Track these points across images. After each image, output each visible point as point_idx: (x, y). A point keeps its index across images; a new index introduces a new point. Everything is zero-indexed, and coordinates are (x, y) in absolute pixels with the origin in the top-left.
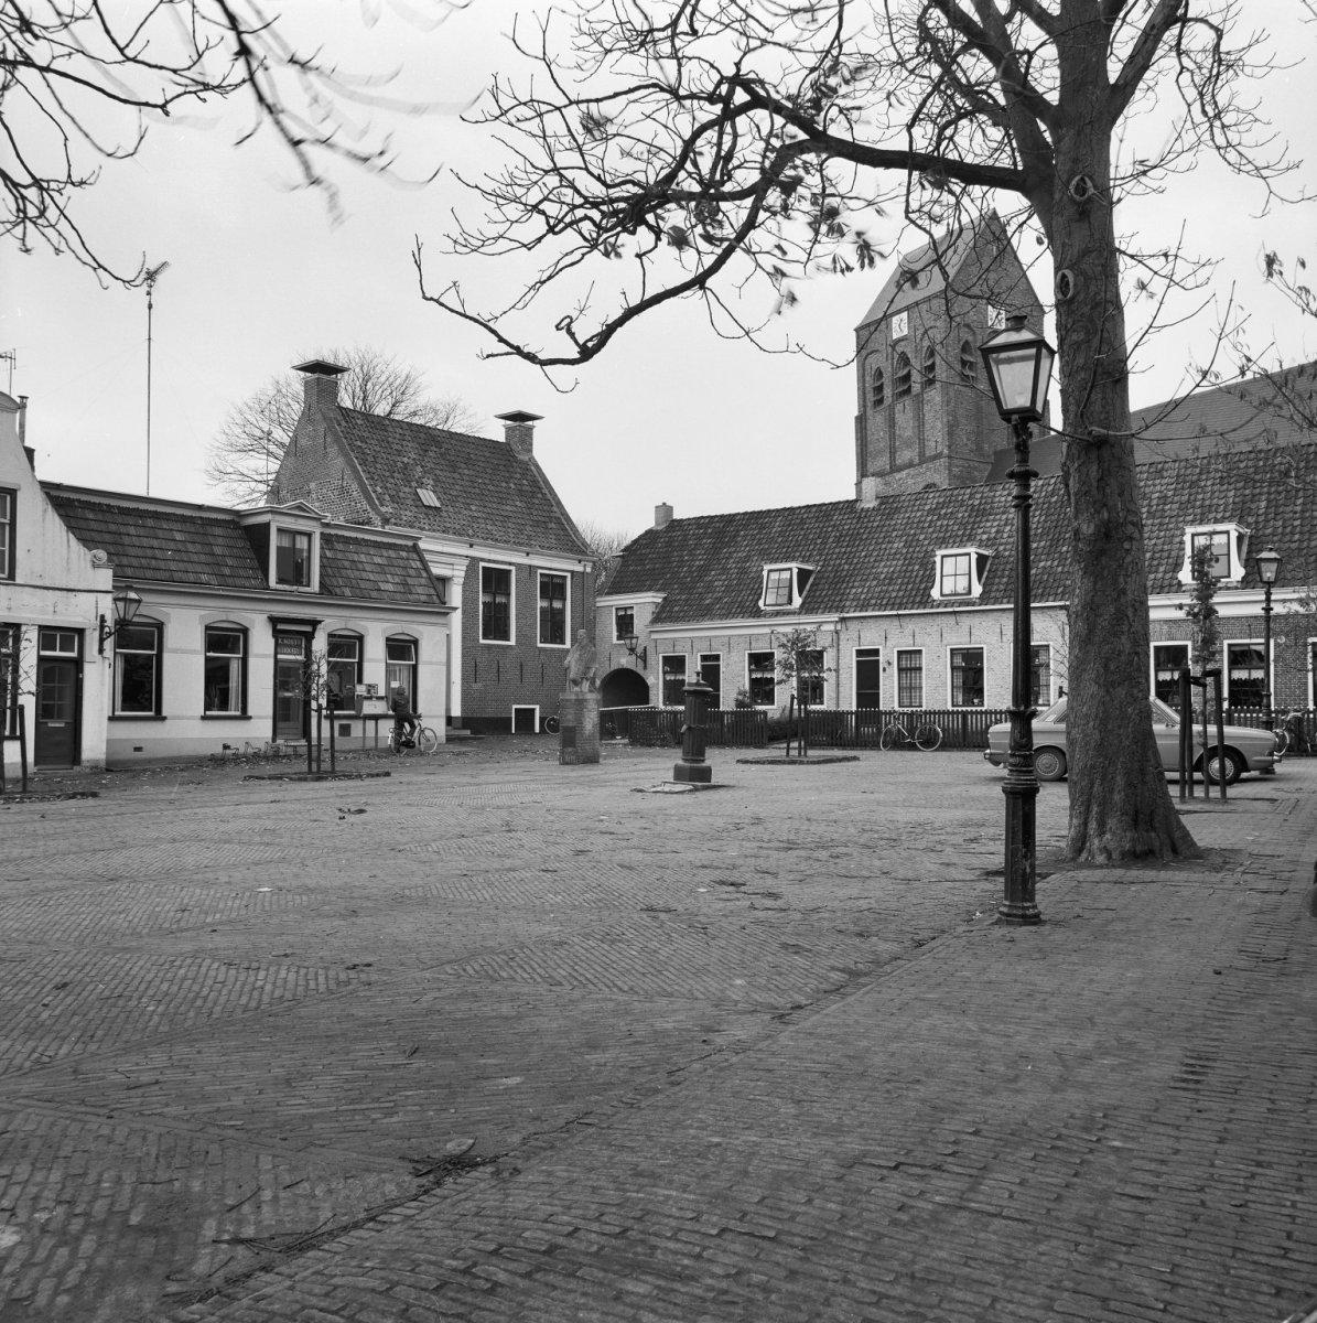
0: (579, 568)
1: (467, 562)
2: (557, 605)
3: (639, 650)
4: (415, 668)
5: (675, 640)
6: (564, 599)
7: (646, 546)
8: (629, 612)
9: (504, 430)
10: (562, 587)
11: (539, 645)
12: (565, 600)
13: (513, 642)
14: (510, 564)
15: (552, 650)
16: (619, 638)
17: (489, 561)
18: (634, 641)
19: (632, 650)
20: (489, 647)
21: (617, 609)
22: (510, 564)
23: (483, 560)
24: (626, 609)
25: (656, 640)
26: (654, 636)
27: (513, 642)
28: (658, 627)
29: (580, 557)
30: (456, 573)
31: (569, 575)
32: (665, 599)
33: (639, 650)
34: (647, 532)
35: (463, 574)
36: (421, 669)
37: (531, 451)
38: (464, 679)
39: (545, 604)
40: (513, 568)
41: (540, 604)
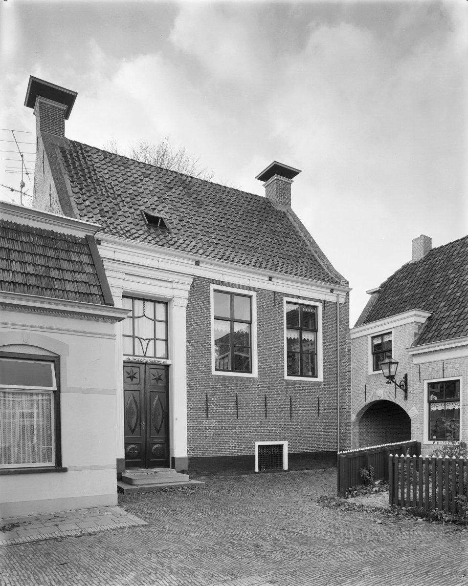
0: (331, 298)
1: (190, 280)
2: (307, 336)
3: (399, 379)
4: (57, 394)
5: (443, 362)
6: (315, 331)
7: (404, 278)
8: (386, 339)
9: (264, 189)
10: (313, 316)
11: (287, 378)
12: (316, 331)
13: (255, 374)
14: (250, 288)
15: (302, 383)
16: (376, 367)
17: (222, 283)
18: (393, 367)
19: (391, 378)
20: (224, 379)
21: (373, 338)
22: (250, 288)
23: (214, 282)
24: (382, 336)
25: (419, 365)
26: (417, 360)
27: (255, 374)
28: (424, 348)
29: (333, 286)
30: (176, 293)
31: (320, 305)
32: (429, 318)
33: (399, 379)
34: (404, 267)
35: (187, 295)
36: (64, 397)
37: (289, 204)
38: (191, 417)
39: (294, 335)
40: (254, 294)
41: (288, 334)
